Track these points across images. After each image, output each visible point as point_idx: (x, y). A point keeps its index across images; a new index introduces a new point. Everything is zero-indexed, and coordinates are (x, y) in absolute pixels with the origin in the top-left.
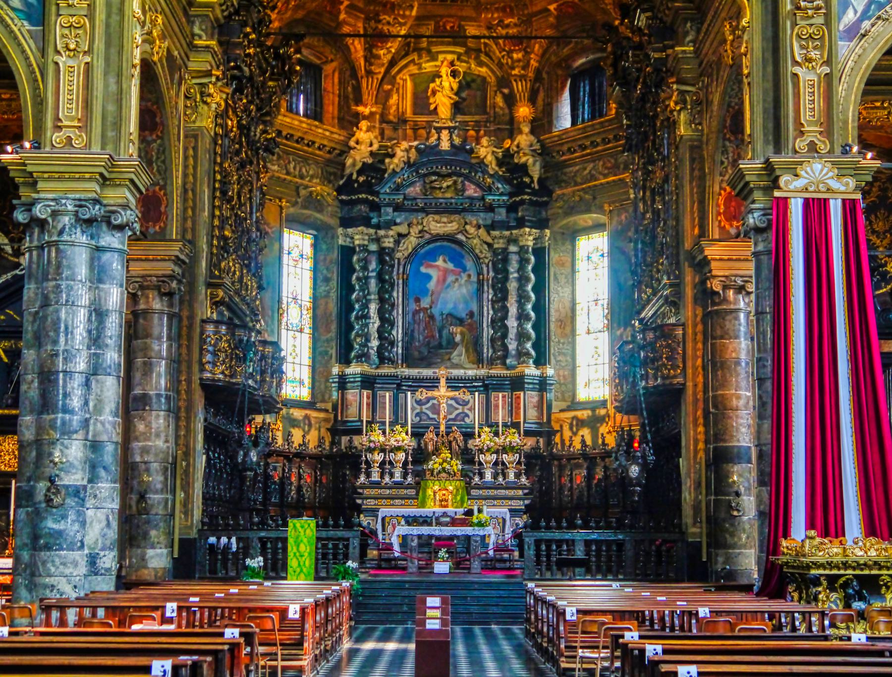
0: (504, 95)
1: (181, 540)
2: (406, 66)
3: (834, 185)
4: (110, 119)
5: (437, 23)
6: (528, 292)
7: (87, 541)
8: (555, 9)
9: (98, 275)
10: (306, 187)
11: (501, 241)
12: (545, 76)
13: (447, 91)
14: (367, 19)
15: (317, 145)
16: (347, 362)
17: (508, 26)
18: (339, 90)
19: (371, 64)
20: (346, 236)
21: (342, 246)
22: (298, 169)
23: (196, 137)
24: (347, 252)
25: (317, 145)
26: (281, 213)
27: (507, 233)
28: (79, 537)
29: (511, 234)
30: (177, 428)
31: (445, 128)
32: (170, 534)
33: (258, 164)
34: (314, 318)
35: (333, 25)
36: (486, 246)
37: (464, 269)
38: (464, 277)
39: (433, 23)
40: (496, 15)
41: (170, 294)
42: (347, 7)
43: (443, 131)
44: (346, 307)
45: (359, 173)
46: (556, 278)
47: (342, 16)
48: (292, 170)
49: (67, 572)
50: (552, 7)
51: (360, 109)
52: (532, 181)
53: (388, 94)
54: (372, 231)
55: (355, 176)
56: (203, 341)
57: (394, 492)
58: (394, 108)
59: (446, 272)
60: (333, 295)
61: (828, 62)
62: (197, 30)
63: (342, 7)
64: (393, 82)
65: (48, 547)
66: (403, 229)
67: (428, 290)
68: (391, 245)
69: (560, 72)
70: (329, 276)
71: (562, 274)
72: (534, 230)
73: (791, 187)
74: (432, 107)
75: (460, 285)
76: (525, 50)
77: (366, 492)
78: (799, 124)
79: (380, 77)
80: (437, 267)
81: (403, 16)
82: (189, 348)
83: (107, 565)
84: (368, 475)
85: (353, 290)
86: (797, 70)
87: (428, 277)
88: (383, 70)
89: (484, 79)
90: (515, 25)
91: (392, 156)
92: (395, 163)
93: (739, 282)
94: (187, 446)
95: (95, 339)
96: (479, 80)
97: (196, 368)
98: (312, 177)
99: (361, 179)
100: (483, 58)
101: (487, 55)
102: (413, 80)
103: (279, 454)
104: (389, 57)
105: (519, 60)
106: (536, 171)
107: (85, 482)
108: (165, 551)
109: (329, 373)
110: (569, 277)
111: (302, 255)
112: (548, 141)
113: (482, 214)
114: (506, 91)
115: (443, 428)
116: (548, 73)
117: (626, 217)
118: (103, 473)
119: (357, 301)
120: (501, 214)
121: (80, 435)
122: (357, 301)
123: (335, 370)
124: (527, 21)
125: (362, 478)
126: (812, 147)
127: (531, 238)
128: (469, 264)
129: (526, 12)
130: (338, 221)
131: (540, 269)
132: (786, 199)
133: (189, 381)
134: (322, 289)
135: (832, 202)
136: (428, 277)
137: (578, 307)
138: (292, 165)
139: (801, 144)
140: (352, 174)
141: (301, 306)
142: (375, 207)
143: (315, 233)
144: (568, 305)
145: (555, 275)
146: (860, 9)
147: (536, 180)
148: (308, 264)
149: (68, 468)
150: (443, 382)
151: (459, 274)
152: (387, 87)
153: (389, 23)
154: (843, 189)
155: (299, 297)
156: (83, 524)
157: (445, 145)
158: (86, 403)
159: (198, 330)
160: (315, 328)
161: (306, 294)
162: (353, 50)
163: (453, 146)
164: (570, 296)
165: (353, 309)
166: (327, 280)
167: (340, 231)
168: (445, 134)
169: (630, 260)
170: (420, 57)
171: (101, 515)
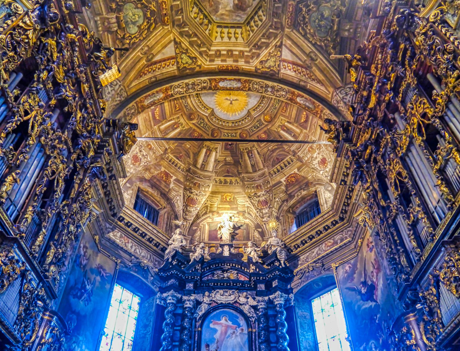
0: (259, 231)
2: (205, 219)
5: (222, 196)
6: (284, 334)
8: (285, 181)
10: (137, 258)
11: (263, 303)
12: (281, 218)
13: (228, 227)
14: (185, 189)
15: (148, 237)
17: (259, 196)
18: (167, 221)
19: (186, 215)
20: (161, 299)
22: (134, 248)
24: (160, 309)
25: (148, 237)
26: (116, 267)
27: (266, 298)
29: (269, 298)
31: (227, 245)
33: (84, 176)
35: (167, 190)
36: (252, 310)
37: (239, 326)
38: (239, 330)
39: (220, 196)
40: (253, 191)
42: (175, 180)
43: (225, 247)
45: (173, 257)
46: (301, 326)
47: (172, 185)
48: (129, 247)
50: (282, 180)
51: (177, 222)
52: (280, 264)
53: (195, 231)
54: (179, 296)
55: (170, 260)
58: (198, 237)
59: (228, 327)
60: (149, 336)
63: (172, 180)
64: (198, 226)
67: (215, 339)
68: (191, 306)
69: (289, 215)
70: (147, 323)
71: (305, 323)
72: (284, 295)
74: (219, 236)
75: (236, 336)
76: (269, 207)
79: (191, 222)
80: (221, 324)
81: (205, 191)
85: (163, 332)
87: (215, 331)
88: (192, 219)
89: (247, 225)
90: (263, 195)
91: (194, 252)
96: (245, 226)
98: (143, 257)
99: (174, 263)
100: (247, 215)
101: (249, 213)
102: (209, 225)
104: (197, 212)
105: (266, 213)
106: (282, 257)
110: (310, 325)
111: (131, 307)
112: (288, 241)
113: (249, 292)
114: (260, 230)
116: (282, 216)
117: (350, 267)
119: (164, 339)
120: (262, 287)
122: (164, 339)
124: (269, 191)
127: (282, 299)
128: (242, 322)
129: (269, 186)
130: (158, 289)
131: (290, 319)
136: (215, 331)
137: (320, 345)
138: (130, 245)
140: (168, 259)
141: (123, 341)
143: (142, 296)
144: (312, 344)
145: (301, 323)
147: (282, 262)
151: (236, 329)
152: (194, 228)
153: (197, 195)
155: (123, 334)
157: (226, 253)
161: (130, 334)
162: (177, 206)
163: (230, 253)
164: (313, 338)
165: (161, 345)
167: (159, 294)
168: (226, 248)
169: (360, 292)
170: (213, 215)
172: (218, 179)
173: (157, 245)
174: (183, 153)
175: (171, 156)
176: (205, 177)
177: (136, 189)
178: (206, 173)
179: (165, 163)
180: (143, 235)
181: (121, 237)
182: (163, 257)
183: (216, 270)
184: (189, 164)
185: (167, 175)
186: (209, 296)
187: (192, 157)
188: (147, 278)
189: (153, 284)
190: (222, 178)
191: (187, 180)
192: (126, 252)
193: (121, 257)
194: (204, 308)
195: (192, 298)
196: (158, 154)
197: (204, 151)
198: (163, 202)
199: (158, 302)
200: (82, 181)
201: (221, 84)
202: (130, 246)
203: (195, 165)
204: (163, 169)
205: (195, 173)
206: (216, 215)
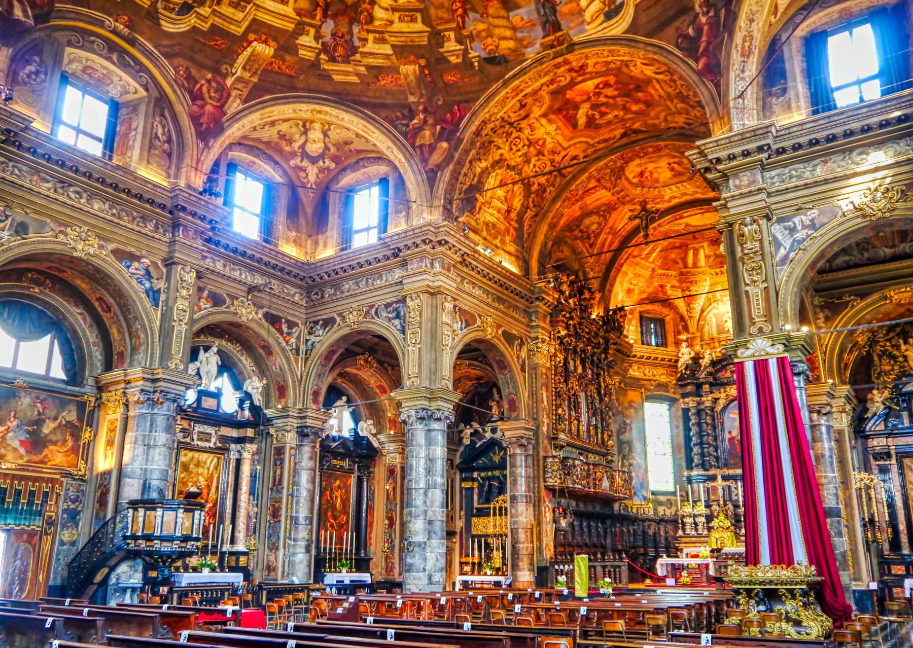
1: (538, 567)
3: (770, 350)
4: (433, 371)
7: (427, 568)
9: (430, 442)
10: (655, 381)
14: (683, 291)
16: (690, 467)
20: (684, 403)
21: (683, 409)
23: (535, 368)
24: (686, 411)
28: (422, 566)
30: (534, 511)
32: (532, 564)
34: (673, 447)
41: (522, 446)
44: (688, 439)
45: (686, 369)
47: (669, 292)
49: (416, 582)
53: (703, 326)
56: (545, 467)
57: (698, 539)
60: (682, 434)
61: (765, 281)
62: (533, 318)
65: (408, 571)
66: (716, 395)
73: (744, 355)
77: (683, 539)
78: (751, 319)
82: (538, 471)
83: (437, 580)
84: (684, 530)
86: (748, 288)
88: (698, 315)
91: (703, 358)
92: (705, 362)
93: (817, 408)
94: (539, 519)
95: (429, 471)
97: (541, 480)
103: (650, 520)
104: (700, 307)
107: (425, 540)
108: (528, 573)
109: (683, 476)
115: (722, 502)
118: (433, 535)
121: (422, 517)
123: (686, 474)
125: (680, 533)
126: (760, 330)
132: (742, 363)
133: (539, 487)
134: (675, 431)
135: (770, 361)
139: (754, 330)
142: (699, 386)
146: (788, 247)
148: (668, 419)
149: (417, 533)
150: (719, 477)
152: (702, 323)
154: (776, 352)
156: (425, 559)
158: (425, 502)
159: (541, 461)
160: (673, 452)
166: (677, 427)
167: (681, 400)
171: (433, 555)
172: (713, 271)
173: (670, 360)
174: (671, 263)
175: (661, 271)
176: (700, 273)
177: (637, 316)
178: (700, 270)
179: (656, 279)
180: (656, 359)
181: (639, 368)
182: (676, 367)
183: (728, 365)
184: (680, 269)
185: (662, 286)
186: (725, 392)
187: (680, 261)
188: (668, 392)
189: (674, 393)
190: (718, 270)
191: (680, 281)
192: (645, 380)
193: (643, 386)
194: (722, 403)
195: (709, 398)
196: (647, 277)
197: (691, 253)
198: (666, 311)
199: (682, 406)
200: (604, 379)
201: (685, 215)
202: (649, 372)
203: (686, 266)
204: (656, 284)
205: (688, 273)
206: (720, 303)
